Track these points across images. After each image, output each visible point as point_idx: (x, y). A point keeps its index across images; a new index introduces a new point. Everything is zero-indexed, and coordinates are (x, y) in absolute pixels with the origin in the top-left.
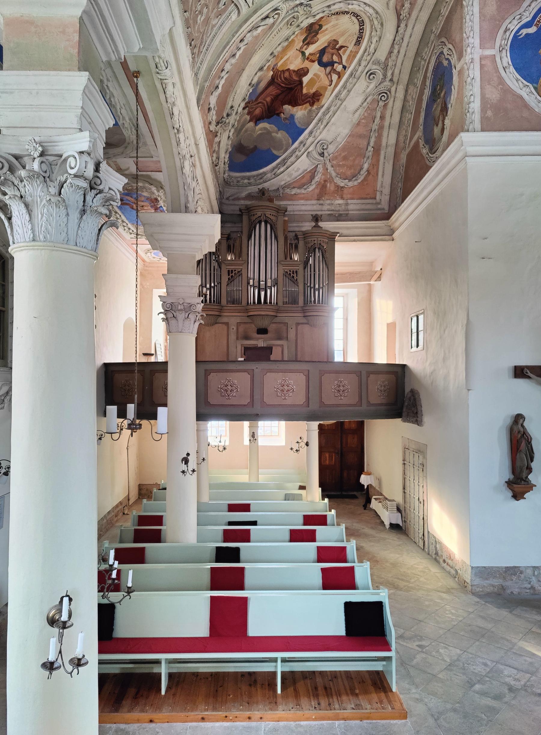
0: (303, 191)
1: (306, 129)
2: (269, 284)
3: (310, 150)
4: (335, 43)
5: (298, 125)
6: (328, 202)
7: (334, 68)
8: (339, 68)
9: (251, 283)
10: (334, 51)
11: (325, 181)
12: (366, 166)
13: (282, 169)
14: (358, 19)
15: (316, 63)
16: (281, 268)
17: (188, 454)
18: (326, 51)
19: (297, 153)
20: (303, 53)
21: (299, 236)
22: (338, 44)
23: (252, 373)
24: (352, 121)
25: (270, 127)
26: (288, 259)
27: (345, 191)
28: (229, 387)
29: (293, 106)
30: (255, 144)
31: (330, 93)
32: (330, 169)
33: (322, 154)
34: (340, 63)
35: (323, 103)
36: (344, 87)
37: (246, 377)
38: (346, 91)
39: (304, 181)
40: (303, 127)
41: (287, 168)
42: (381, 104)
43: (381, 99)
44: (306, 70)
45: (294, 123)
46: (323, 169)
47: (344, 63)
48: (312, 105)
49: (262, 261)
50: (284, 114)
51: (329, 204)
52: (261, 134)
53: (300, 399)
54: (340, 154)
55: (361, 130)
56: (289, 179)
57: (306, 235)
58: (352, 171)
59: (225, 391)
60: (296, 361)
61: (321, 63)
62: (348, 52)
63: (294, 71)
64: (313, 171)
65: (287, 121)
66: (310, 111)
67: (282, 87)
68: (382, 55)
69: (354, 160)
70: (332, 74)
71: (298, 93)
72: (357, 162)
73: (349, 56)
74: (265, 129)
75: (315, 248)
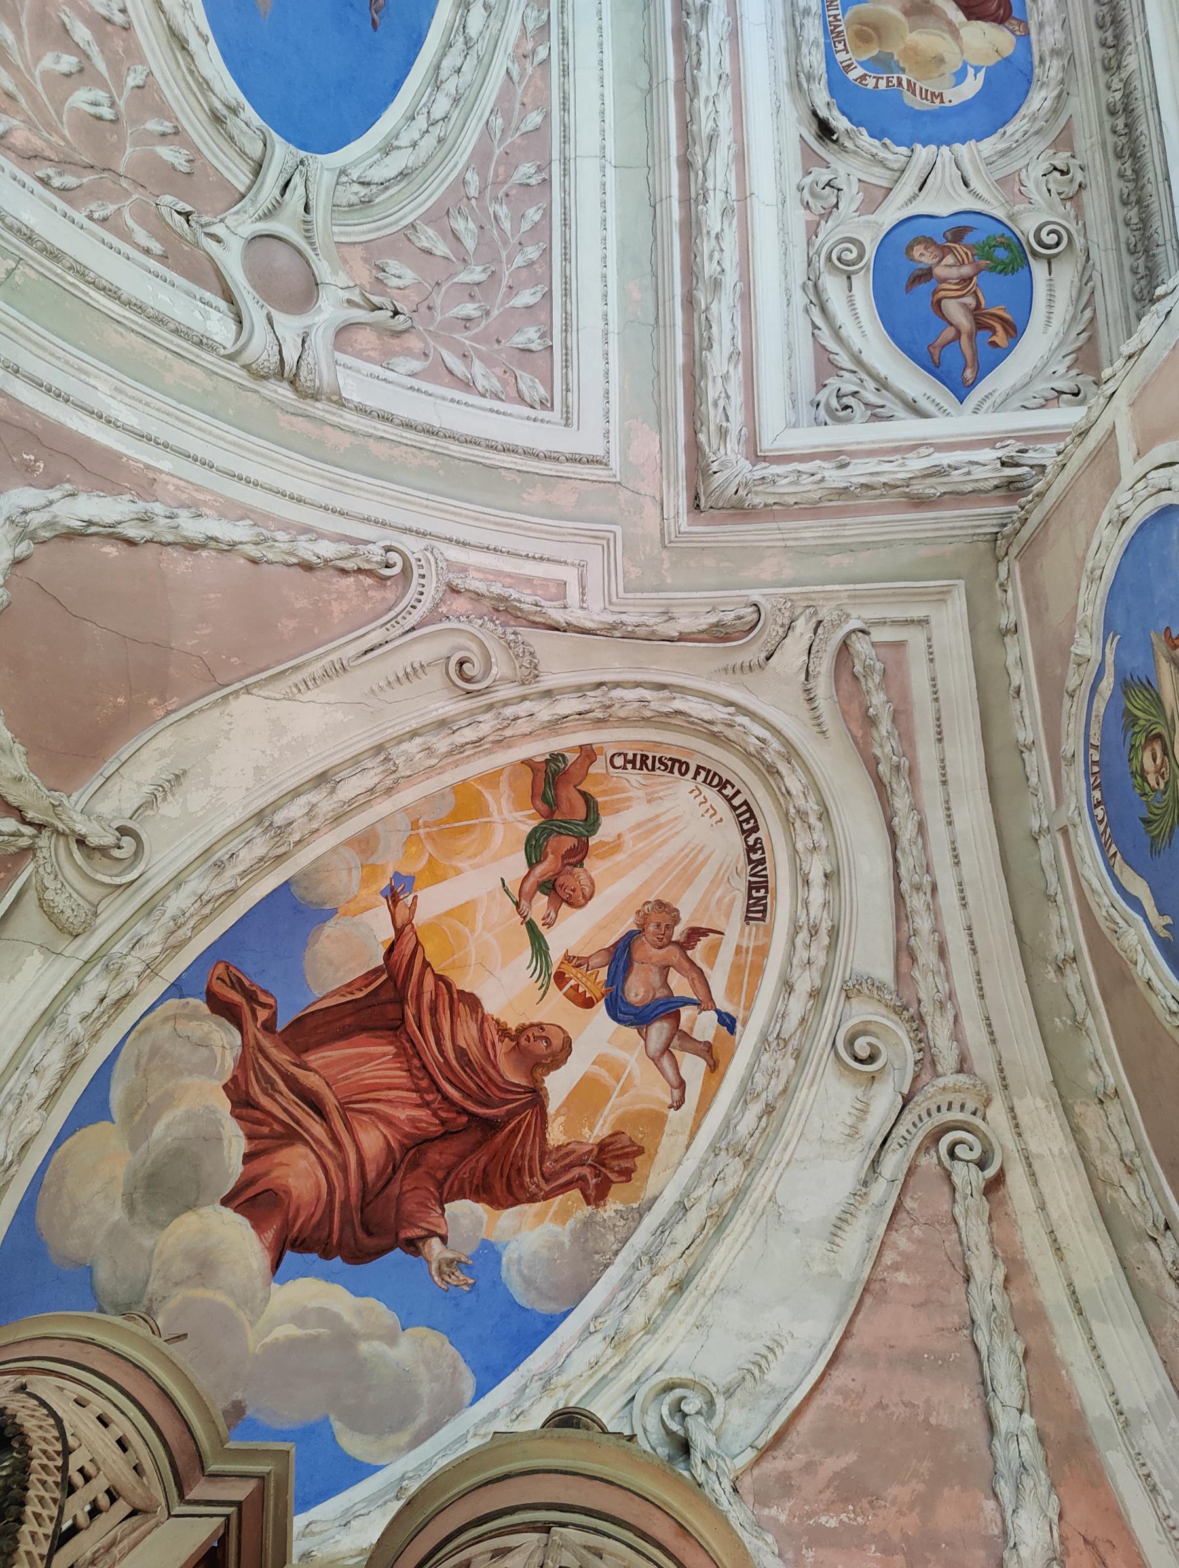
4: (665, 919)
7: (684, 1024)
8: (704, 1026)
10: (673, 954)
14: (729, 800)
15: (601, 1007)
18: (637, 955)
20: (539, 947)
22: (676, 920)
24: (835, 1274)
25: (358, 1312)
29: (497, 1203)
30: (238, 1395)
31: (683, 1139)
34: (705, 1002)
35: (649, 1192)
36: (746, 1093)
40: (547, 1307)
42: (967, 1177)
43: (952, 1154)
44: (557, 1043)
45: (497, 1282)
47: (721, 1001)
48: (597, 1196)
50: (444, 1239)
52: (292, 1344)
54: (809, 1468)
61: (619, 1010)
62: (726, 955)
63: (503, 1032)
66: (588, 1223)
67: (446, 1098)
68: (870, 951)
69: (925, 1504)
71: (523, 1144)
72: (947, 1517)
73: (737, 969)
74: (324, 1316)
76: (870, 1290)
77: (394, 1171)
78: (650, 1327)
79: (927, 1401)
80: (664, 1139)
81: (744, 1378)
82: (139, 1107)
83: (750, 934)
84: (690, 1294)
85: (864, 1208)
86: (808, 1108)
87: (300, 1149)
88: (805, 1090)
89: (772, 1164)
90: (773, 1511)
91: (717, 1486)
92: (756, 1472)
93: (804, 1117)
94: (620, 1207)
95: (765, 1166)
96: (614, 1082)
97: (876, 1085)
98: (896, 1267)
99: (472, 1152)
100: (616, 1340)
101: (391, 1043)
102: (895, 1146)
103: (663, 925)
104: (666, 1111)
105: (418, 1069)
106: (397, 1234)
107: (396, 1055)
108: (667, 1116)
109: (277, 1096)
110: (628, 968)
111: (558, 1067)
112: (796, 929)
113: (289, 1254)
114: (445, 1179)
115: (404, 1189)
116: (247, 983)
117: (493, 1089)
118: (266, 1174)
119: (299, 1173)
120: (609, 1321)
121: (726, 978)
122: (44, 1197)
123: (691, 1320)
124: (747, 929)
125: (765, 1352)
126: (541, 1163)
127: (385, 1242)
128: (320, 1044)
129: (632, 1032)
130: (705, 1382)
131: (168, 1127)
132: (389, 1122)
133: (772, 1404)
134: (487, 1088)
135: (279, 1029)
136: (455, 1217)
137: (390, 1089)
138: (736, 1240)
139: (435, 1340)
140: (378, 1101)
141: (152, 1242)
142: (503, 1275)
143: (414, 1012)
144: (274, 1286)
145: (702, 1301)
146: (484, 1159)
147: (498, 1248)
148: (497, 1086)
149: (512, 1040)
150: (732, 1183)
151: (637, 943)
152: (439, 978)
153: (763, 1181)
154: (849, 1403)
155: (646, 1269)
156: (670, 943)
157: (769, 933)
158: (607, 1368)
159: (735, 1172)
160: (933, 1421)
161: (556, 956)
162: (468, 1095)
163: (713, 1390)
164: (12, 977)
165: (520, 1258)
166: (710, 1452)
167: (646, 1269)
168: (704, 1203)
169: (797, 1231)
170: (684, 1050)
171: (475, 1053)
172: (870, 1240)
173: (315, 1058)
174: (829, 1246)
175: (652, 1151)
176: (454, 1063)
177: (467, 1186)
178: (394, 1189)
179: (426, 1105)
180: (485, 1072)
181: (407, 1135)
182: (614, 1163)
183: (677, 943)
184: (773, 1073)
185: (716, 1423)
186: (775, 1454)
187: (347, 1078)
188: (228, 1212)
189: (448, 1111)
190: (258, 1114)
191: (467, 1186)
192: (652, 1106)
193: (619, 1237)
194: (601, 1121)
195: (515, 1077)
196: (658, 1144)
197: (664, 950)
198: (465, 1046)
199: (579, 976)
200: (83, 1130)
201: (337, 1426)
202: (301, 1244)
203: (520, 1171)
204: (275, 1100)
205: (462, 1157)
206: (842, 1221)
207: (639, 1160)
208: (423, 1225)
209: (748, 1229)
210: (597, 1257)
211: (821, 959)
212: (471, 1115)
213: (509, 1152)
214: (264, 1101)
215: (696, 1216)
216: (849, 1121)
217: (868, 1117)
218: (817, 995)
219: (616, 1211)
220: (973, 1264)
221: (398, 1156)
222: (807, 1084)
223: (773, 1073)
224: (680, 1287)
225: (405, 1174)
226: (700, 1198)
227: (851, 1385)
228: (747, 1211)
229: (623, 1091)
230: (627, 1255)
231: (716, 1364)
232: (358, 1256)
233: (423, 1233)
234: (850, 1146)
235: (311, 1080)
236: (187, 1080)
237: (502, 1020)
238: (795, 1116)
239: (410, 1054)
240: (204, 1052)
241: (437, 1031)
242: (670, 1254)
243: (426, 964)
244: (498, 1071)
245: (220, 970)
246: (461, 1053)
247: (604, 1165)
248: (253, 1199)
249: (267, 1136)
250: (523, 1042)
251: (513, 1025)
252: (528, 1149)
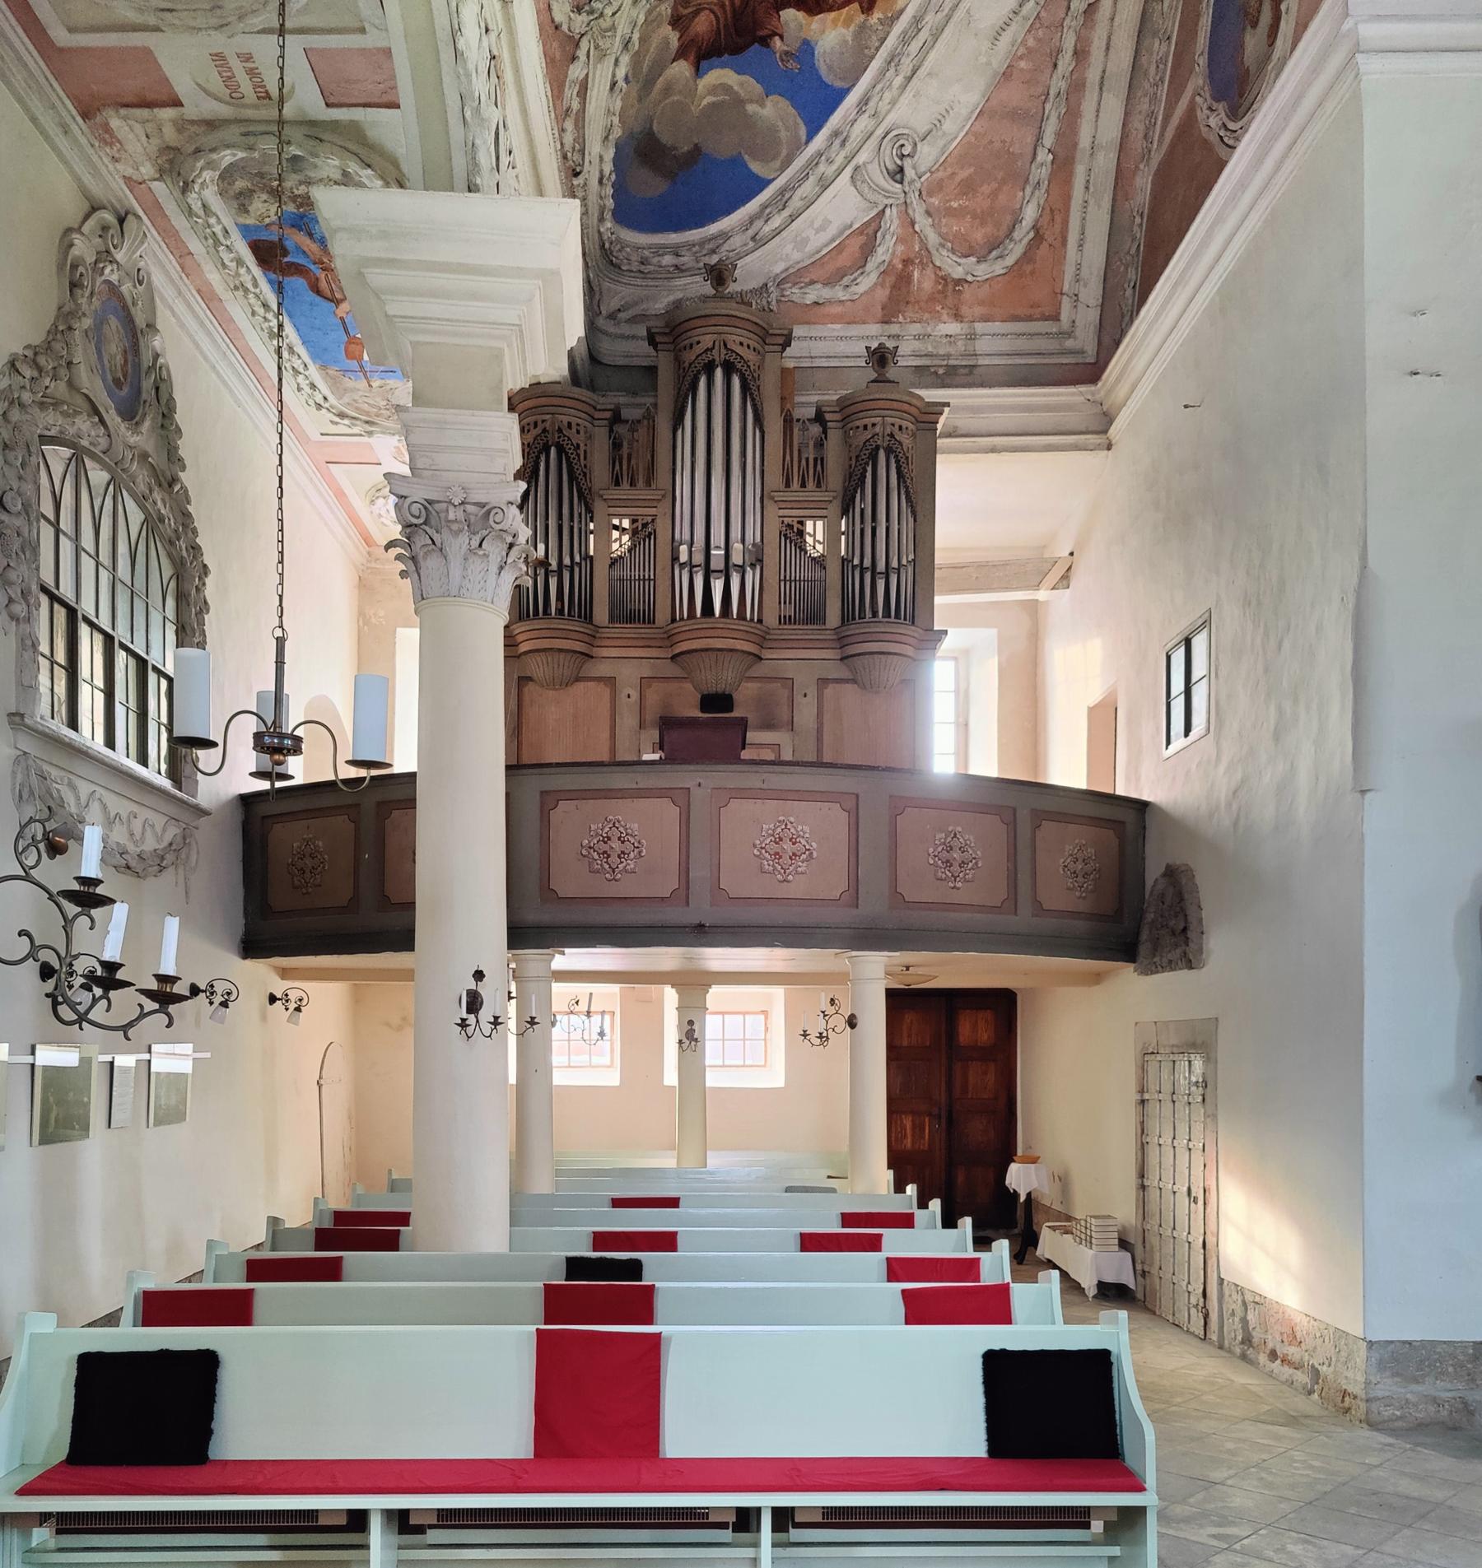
0: (839, 293)
1: (848, 90)
2: (737, 558)
3: (861, 158)
6: (916, 328)
9: (684, 558)
11: (907, 262)
12: (1030, 213)
13: (776, 222)
16: (772, 511)
17: (479, 975)
19: (822, 168)
21: (828, 417)
23: (681, 798)
25: (741, 84)
26: (795, 485)
27: (968, 292)
28: (616, 844)
32: (923, 223)
33: (898, 174)
37: (669, 812)
39: (844, 260)
40: (838, 84)
41: (793, 218)
46: (902, 225)
49: (719, 506)
50: (781, 37)
51: (917, 337)
52: (713, 106)
53: (834, 884)
55: (1015, 95)
56: (796, 256)
57: (848, 411)
58: (989, 229)
59: (603, 854)
60: (819, 764)
64: (870, 231)
65: (792, 65)
66: (863, 27)
74: (726, 88)
75: (878, 448)
76: (1007, 75)
98: (1021, 58)
139: (784, 104)
201: (746, 157)
220: (1060, 63)
230: (883, 53)
232: (736, 50)
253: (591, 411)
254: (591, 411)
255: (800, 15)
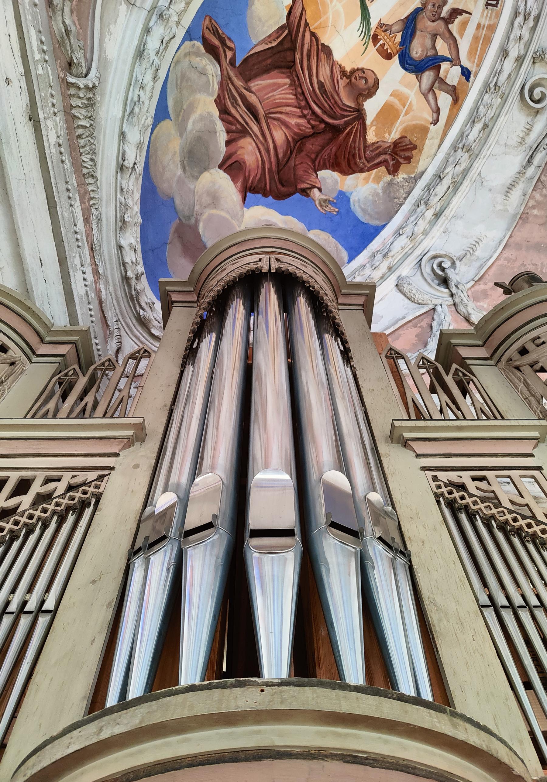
1: (384, 226)
3: (406, 270)
5: (363, 220)
7: (442, 74)
10: (440, 25)
15: (396, 59)
18: (419, 26)
24: (506, 210)
25: (285, 222)
29: (344, 173)
31: (437, 141)
34: (455, 61)
35: (420, 169)
38: (479, 126)
44: (371, 81)
45: (349, 211)
48: (394, 170)
50: (320, 189)
62: (471, 30)
63: (343, 72)
66: (390, 184)
67: (314, 113)
70: (437, 91)
71: (354, 141)
73: (476, 39)
76: (523, 218)
77: (291, 153)
78: (425, 233)
79: (542, 263)
80: (427, 142)
81: (466, 254)
82: (180, 111)
83: (487, 16)
84: (442, 218)
85: (522, 179)
86: (502, 127)
87: (248, 140)
88: (503, 117)
89: (482, 157)
90: (481, 304)
91: (462, 295)
92: (473, 289)
93: (499, 132)
94: (405, 176)
95: (479, 157)
96: (402, 107)
97: (538, 115)
98: (533, 207)
99: (328, 144)
100: (412, 237)
101: (288, 77)
102: (542, 149)
103: (437, 5)
104: (429, 125)
105: (300, 94)
106: (296, 186)
107: (291, 85)
108: (429, 128)
109: (238, 108)
110: (413, 35)
111: (371, 97)
112: (516, 14)
113: (249, 194)
114: (316, 158)
115: (297, 163)
116: (221, 32)
117: (338, 109)
118: (236, 153)
119: (249, 151)
120: (408, 230)
121: (469, 45)
122: (151, 161)
123: (442, 230)
124: (486, 11)
125: (475, 243)
126: (365, 152)
127: (291, 190)
128: (256, 76)
129: (412, 77)
130: (451, 256)
131: (193, 124)
132: (286, 124)
133: (478, 264)
134: (334, 109)
135: (237, 65)
136: (324, 179)
137: (287, 106)
138: (462, 194)
140: (281, 113)
141: (194, 186)
142: (352, 207)
143: (300, 57)
144: (245, 209)
145: (446, 222)
146: (334, 149)
147: (348, 194)
148: (339, 107)
149: (347, 78)
150: (463, 167)
151: (420, 17)
152: (313, 34)
153: (477, 165)
154: (509, 264)
155: (423, 207)
156: (440, 18)
157: (498, 16)
158: (408, 249)
159: (465, 160)
160: (544, 271)
161: (374, 23)
162: (324, 112)
163: (455, 258)
164: (116, 21)
165: (359, 200)
166: (459, 283)
167: (423, 207)
168: (450, 176)
169: (490, 190)
170: (440, 89)
171: (328, 86)
172: (525, 195)
173: (255, 84)
174: (504, 197)
175: (421, 148)
176: (318, 91)
177: (327, 163)
178: (292, 163)
179: (304, 116)
180: (333, 98)
181: (295, 133)
182: (402, 153)
183: (443, 19)
184: (490, 106)
185: (457, 271)
186: (480, 283)
187: (268, 98)
188: (221, 172)
189: (315, 120)
190: (231, 119)
191: (327, 163)
192: (422, 123)
193: (406, 191)
194: (395, 130)
195: (349, 102)
196: (424, 144)
197: (436, 23)
198: (323, 81)
199: (386, 37)
200: (160, 124)
202: (253, 189)
203: (354, 156)
204: (237, 110)
205: (323, 147)
206: (512, 186)
207: (414, 152)
208: (308, 182)
209: (468, 189)
210: (396, 200)
211: (526, 35)
212: (327, 124)
213: (347, 145)
214: (233, 111)
215: (447, 182)
216: (521, 135)
217: (531, 133)
218: (520, 60)
219: (403, 178)
221: (292, 145)
222: (504, 115)
223: (490, 106)
224: (437, 216)
225: (296, 155)
226: (448, 173)
227: (511, 257)
228: (469, 180)
229: (407, 113)
231: (454, 248)
232: (280, 196)
233: (309, 186)
234: (520, 148)
235: (253, 99)
236: (198, 96)
237: (343, 65)
238: (496, 131)
239: (296, 84)
240: (204, 78)
241: (310, 70)
242: (434, 200)
243: (307, 24)
244: (339, 98)
245: (207, 22)
246: (321, 85)
247: (397, 154)
248: (232, 166)
249: (237, 132)
250: (353, 80)
251: (348, 69)
252: (357, 144)
253: (33, 339)
254: (33, 339)
255: (336, 175)
